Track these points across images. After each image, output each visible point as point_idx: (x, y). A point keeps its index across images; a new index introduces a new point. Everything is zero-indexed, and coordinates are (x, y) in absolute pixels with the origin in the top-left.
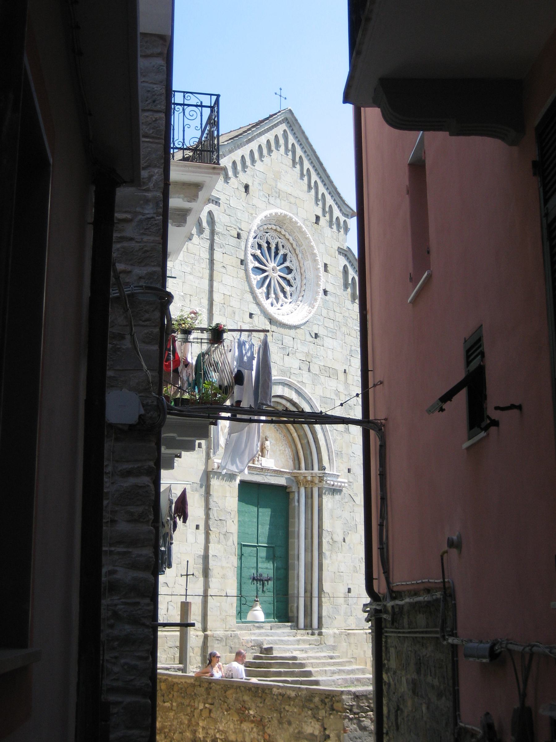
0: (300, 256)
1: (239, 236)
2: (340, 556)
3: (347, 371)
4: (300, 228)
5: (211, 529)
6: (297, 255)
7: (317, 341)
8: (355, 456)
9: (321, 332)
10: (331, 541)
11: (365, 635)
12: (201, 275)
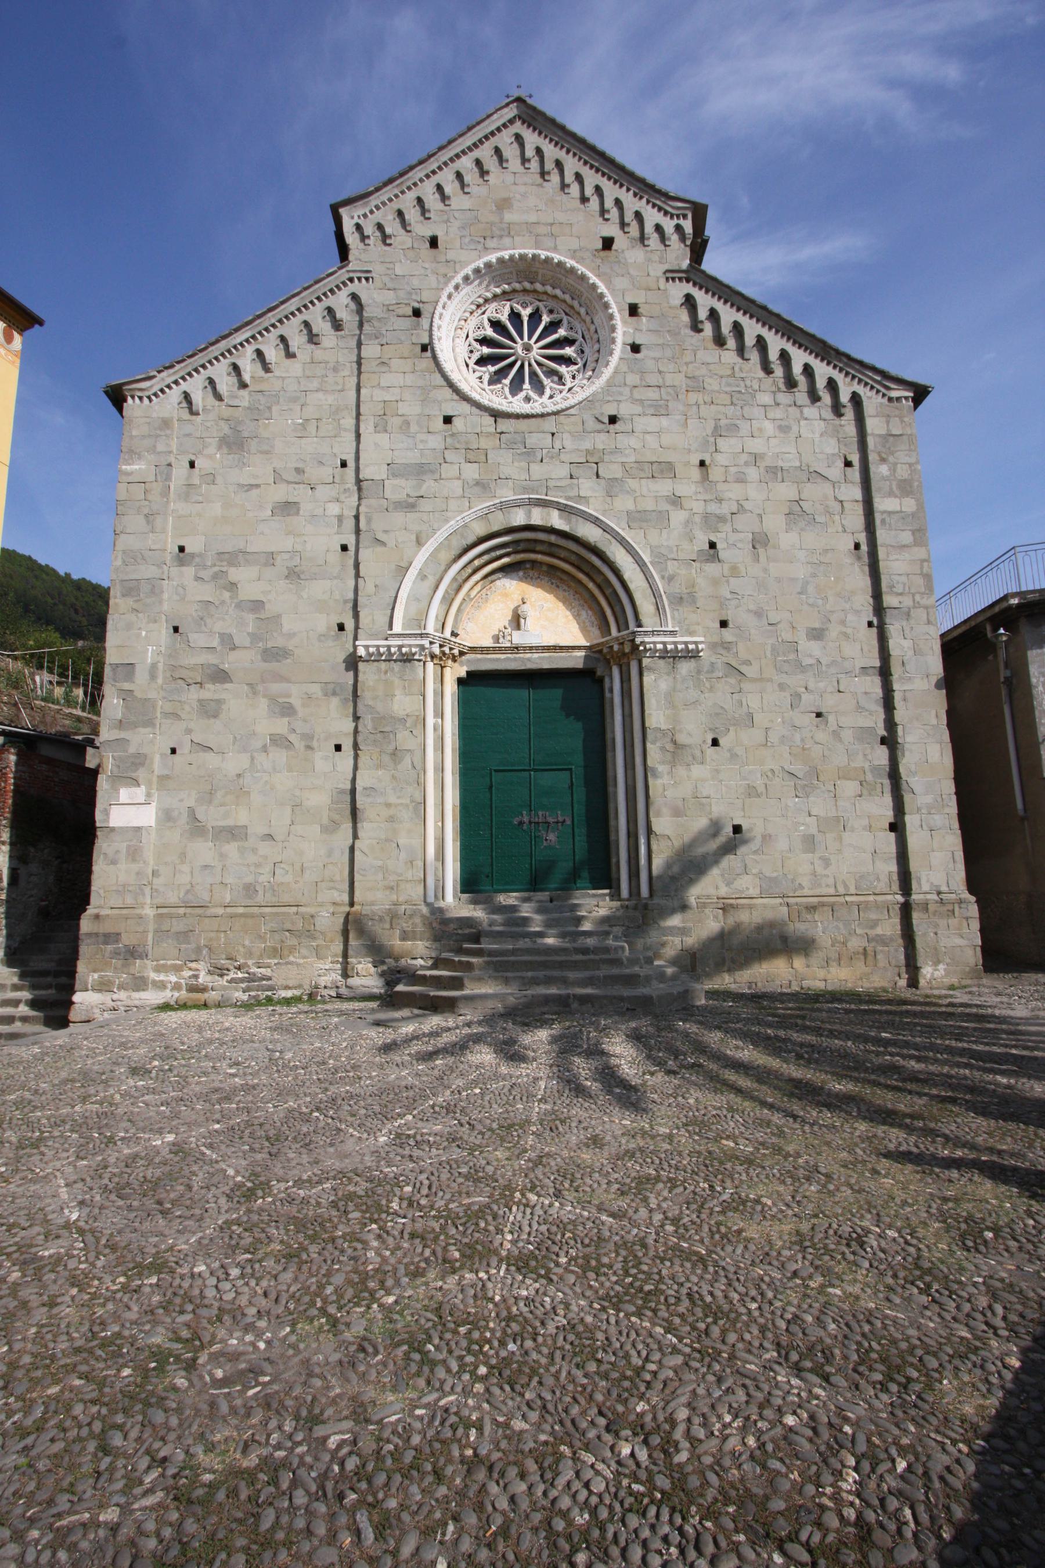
0: (583, 311)
1: (417, 313)
2: (697, 771)
4: (572, 271)
6: (579, 314)
7: (617, 426)
9: (624, 410)
10: (670, 747)
12: (340, 387)
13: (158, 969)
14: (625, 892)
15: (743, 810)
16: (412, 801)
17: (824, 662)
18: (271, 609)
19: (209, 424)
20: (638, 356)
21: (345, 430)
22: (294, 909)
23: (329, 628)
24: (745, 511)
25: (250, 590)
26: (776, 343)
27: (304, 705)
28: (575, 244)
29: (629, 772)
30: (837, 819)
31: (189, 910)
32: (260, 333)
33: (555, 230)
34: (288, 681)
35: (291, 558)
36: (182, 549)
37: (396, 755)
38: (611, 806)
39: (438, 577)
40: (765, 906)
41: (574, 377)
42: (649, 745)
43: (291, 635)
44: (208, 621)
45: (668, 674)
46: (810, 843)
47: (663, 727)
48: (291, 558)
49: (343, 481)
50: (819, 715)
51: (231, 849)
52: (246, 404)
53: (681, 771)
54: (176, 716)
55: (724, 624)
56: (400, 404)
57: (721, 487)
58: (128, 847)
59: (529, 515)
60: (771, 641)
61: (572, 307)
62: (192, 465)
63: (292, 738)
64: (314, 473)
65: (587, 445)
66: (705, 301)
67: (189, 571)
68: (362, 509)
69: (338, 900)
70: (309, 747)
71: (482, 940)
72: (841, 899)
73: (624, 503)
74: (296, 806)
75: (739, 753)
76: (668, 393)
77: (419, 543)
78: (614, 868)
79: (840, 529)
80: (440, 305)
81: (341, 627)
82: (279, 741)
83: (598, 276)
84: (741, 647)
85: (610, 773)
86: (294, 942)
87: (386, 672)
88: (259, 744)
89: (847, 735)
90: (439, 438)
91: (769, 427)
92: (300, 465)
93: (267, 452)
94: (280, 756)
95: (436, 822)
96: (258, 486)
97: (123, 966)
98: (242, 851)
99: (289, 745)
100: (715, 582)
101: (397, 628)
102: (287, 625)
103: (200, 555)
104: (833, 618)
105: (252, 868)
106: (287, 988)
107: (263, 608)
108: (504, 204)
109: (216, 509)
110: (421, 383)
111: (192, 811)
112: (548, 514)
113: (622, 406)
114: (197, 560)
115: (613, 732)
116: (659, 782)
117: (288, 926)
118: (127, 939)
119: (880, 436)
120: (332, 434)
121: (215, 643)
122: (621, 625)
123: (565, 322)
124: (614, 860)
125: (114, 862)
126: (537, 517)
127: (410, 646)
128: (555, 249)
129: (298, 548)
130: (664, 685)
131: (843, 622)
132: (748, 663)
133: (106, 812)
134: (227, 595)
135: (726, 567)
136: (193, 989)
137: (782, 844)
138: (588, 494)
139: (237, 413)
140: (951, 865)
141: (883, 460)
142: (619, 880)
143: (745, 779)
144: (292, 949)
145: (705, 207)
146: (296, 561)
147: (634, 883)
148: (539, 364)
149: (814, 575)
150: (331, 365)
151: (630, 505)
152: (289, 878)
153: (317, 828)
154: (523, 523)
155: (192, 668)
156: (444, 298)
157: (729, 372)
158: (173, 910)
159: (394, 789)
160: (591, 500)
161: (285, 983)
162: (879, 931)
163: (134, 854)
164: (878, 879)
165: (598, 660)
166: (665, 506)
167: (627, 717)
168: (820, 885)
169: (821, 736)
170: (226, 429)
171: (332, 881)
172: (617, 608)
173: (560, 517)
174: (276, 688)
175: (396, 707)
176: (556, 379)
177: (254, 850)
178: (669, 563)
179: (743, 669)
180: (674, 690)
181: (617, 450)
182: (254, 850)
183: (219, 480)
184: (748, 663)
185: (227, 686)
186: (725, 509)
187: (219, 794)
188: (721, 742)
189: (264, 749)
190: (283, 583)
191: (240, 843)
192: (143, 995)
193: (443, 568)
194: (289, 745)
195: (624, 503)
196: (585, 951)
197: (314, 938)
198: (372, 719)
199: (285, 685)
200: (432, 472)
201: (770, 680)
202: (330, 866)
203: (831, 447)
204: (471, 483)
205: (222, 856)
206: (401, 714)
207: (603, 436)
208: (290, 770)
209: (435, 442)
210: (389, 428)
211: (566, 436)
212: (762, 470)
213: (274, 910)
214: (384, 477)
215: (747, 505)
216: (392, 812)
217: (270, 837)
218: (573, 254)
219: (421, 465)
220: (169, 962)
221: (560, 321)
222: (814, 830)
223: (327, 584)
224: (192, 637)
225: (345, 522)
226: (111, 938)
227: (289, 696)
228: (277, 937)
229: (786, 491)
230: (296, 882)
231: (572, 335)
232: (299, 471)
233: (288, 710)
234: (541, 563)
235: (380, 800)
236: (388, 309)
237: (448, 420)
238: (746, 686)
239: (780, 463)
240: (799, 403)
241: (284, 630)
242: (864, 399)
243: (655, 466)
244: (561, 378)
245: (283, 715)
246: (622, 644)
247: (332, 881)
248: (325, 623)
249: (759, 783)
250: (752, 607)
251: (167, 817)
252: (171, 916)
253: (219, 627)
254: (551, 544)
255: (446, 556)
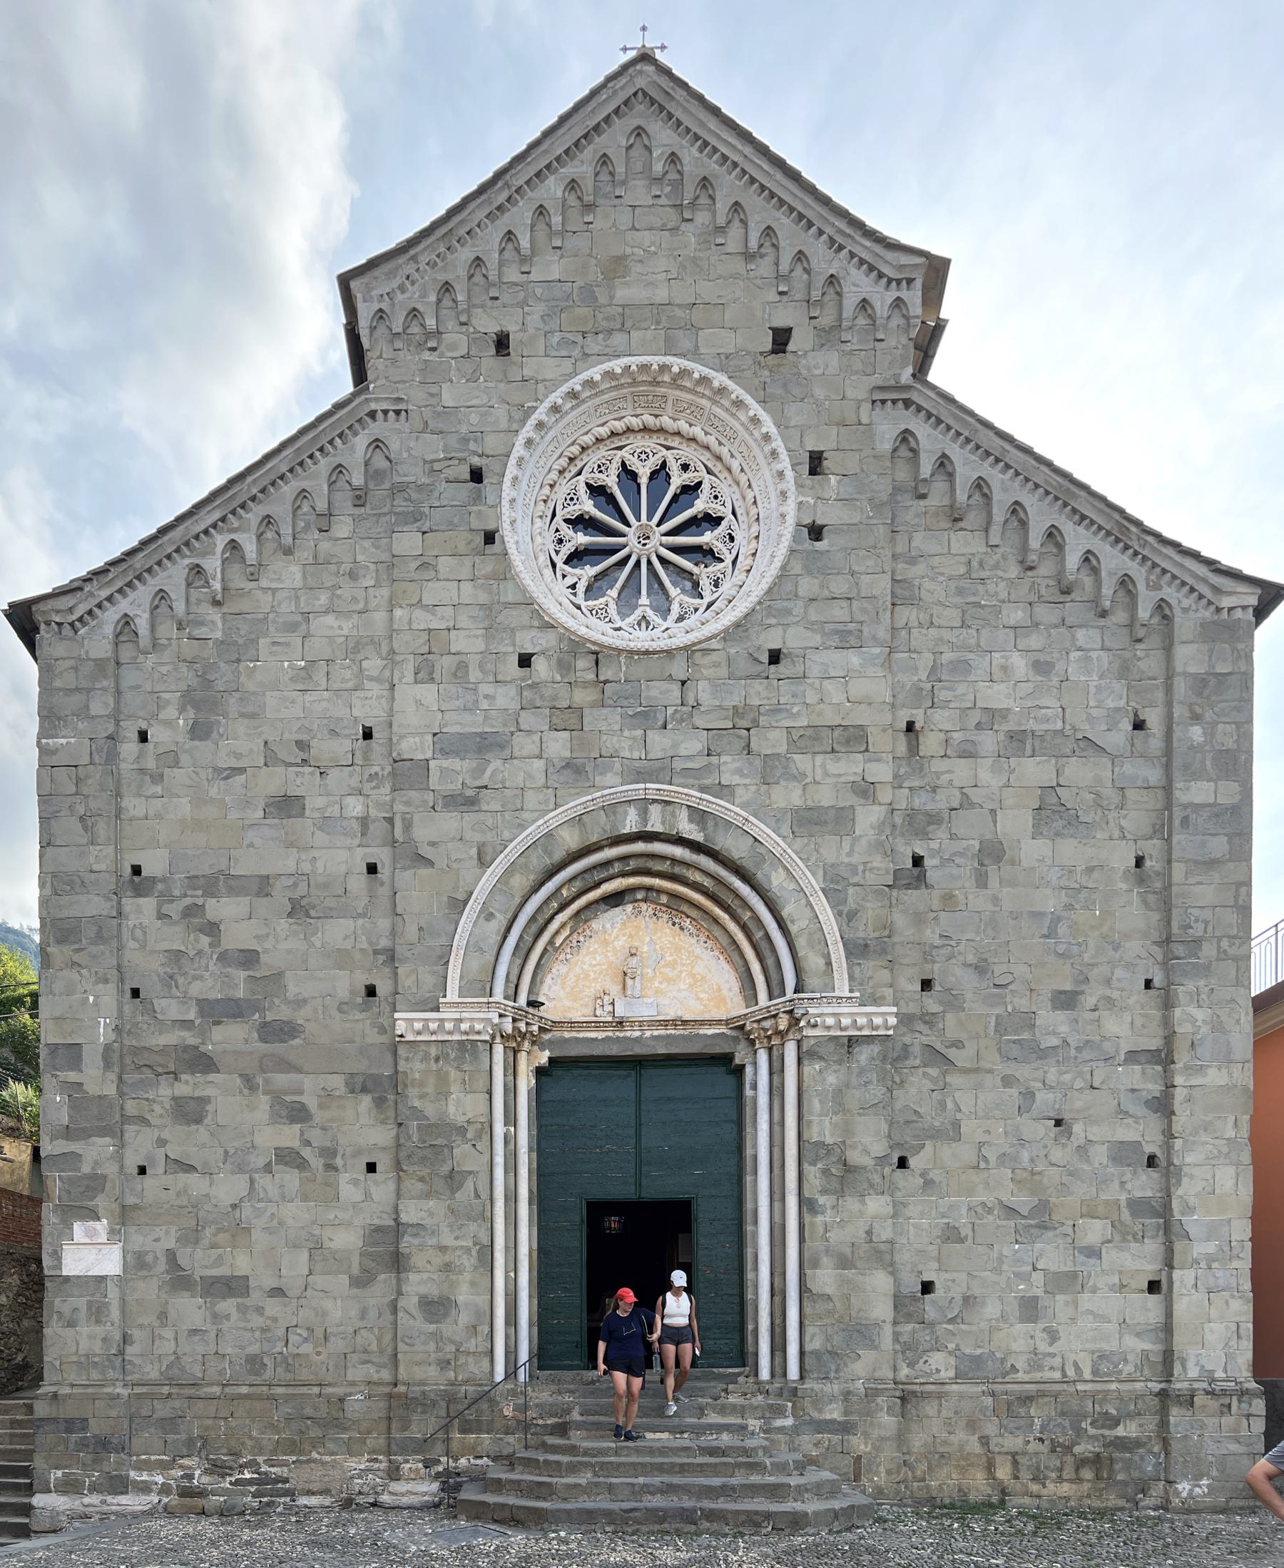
2: (876, 1205)
3: (918, 726)
5: (405, 1168)
7: (782, 669)
8: (953, 943)
11: (990, 1399)
12: (360, 606)
13: (139, 1467)
14: (765, 1374)
15: (939, 1260)
16: (475, 1244)
17: (1073, 1044)
18: (270, 962)
19: (164, 669)
20: (818, 545)
21: (371, 679)
22: (316, 1390)
23: (353, 993)
24: (972, 805)
25: (238, 936)
26: (1040, 516)
27: (321, 1106)
28: (728, 342)
29: (777, 1205)
30: (1073, 1276)
31: (175, 1390)
32: (233, 512)
33: (697, 316)
34: (299, 1070)
35: (295, 885)
36: (137, 870)
37: (454, 1179)
38: (749, 1252)
39: (509, 915)
40: (961, 1396)
41: (716, 585)
42: (806, 1166)
43: (300, 1003)
44: (181, 980)
45: (840, 1062)
46: (1030, 1309)
47: (829, 1140)
48: (295, 885)
49: (366, 757)
50: (1058, 1123)
51: (228, 1306)
52: (218, 635)
53: (851, 1203)
54: (142, 1121)
55: (926, 985)
56: (453, 633)
57: (938, 765)
58: (90, 1303)
59: (644, 814)
60: (997, 1011)
61: (719, 458)
62: (143, 737)
63: (306, 1153)
64: (324, 748)
65: (735, 700)
66: (929, 440)
67: (148, 904)
68: (399, 807)
69: (375, 1377)
70: (330, 1167)
71: (572, 1433)
72: (1071, 1389)
73: (787, 796)
74: (316, 1248)
75: (937, 1180)
76: (864, 610)
77: (483, 862)
78: (750, 1339)
79: (1117, 834)
80: (512, 461)
81: (371, 991)
82: (287, 1158)
83: (762, 402)
84: (950, 1019)
85: (749, 1206)
86: (315, 1432)
87: (437, 1060)
88: (261, 1162)
89: (1100, 1154)
90: (512, 690)
91: (1019, 663)
92: (305, 737)
93: (253, 716)
94: (291, 1178)
95: (506, 1272)
96: (242, 770)
97: (94, 1461)
98: (242, 1309)
99: (302, 1164)
100: (919, 919)
101: (452, 995)
102: (292, 991)
103: (164, 880)
104: (1093, 974)
105: (257, 1334)
106: (310, 1493)
107: (258, 961)
108: (616, 267)
109: (183, 807)
110: (483, 598)
111: (171, 1255)
112: (673, 814)
113: (792, 631)
114: (160, 886)
115: (755, 1146)
116: (819, 1219)
117: (309, 1411)
118: (95, 1428)
119: (1195, 676)
120: (350, 685)
121: (191, 1015)
122: (777, 987)
123: (705, 486)
124: (750, 1327)
125: (71, 1324)
126: (655, 825)
127: (472, 1020)
128: (695, 354)
129: (306, 867)
130: (832, 1079)
131: (1108, 982)
132: (958, 1044)
133: (57, 1256)
134: (205, 940)
135: (936, 894)
136: (185, 1493)
137: (991, 1310)
138: (736, 780)
139: (209, 651)
140: (1233, 1343)
141: (1196, 718)
142: (756, 1354)
143: (943, 1217)
144: (316, 1443)
145: (946, 263)
146: (302, 889)
147: (778, 1360)
148: (663, 561)
149: (1069, 907)
150: (345, 568)
151: (796, 798)
152: (307, 1348)
153: (344, 1279)
154: (634, 830)
155: (164, 1051)
156: (519, 450)
157: (962, 570)
158: (155, 1389)
159: (450, 1226)
160: (739, 791)
161: (307, 1487)
162: (1120, 1431)
163: (98, 1313)
164: (1126, 1361)
165: (736, 1039)
166: (850, 800)
167: (777, 1126)
168: (1040, 1368)
169: (1058, 1155)
170: (193, 681)
171: (366, 1351)
172: (770, 962)
173: (691, 820)
174: (281, 1080)
175: (452, 1109)
176: (688, 585)
177: (260, 1310)
178: (851, 890)
179: (952, 1053)
180: (847, 1086)
181: (776, 711)
182: (260, 1310)
183: (185, 759)
184: (958, 1044)
185: (211, 1077)
186: (941, 802)
187: (208, 1232)
188: (912, 1162)
189: (268, 1168)
190: (283, 925)
191: (239, 1300)
192: (123, 1499)
193: (517, 900)
194: (302, 1164)
195: (787, 796)
196: (712, 1451)
197: (346, 1429)
198: (419, 1127)
199: (293, 1076)
200: (502, 746)
201: (990, 1071)
202: (363, 1332)
203: (1116, 697)
204: (559, 764)
205: (216, 1317)
206: (460, 1120)
207: (758, 685)
208: (305, 1198)
209: (506, 698)
210: (437, 676)
211: (702, 685)
212: (1001, 737)
213: (290, 1391)
214: (429, 755)
215: (976, 796)
216: (447, 1258)
217: (278, 1292)
218: (724, 363)
219: (483, 736)
220: (153, 1458)
221: (700, 484)
222: (1039, 1292)
223: (346, 925)
224: (160, 1004)
225: (371, 827)
226: (71, 1425)
227: (301, 1093)
228: (294, 1426)
229: (1035, 771)
230: (318, 1353)
231: (715, 509)
232: (302, 745)
233: (299, 1114)
234: (659, 891)
235: (432, 1241)
236: (431, 467)
237: (525, 661)
238: (954, 1079)
239: (1031, 725)
240: (1069, 621)
241: (290, 995)
242: (1177, 612)
243: (836, 733)
244: (696, 585)
245: (293, 1119)
246: (775, 1016)
247: (366, 1351)
248: (347, 984)
249: (963, 1221)
250: (971, 959)
251: (137, 1263)
252: (152, 1397)
253: (196, 989)
254: (674, 861)
255: (520, 882)
